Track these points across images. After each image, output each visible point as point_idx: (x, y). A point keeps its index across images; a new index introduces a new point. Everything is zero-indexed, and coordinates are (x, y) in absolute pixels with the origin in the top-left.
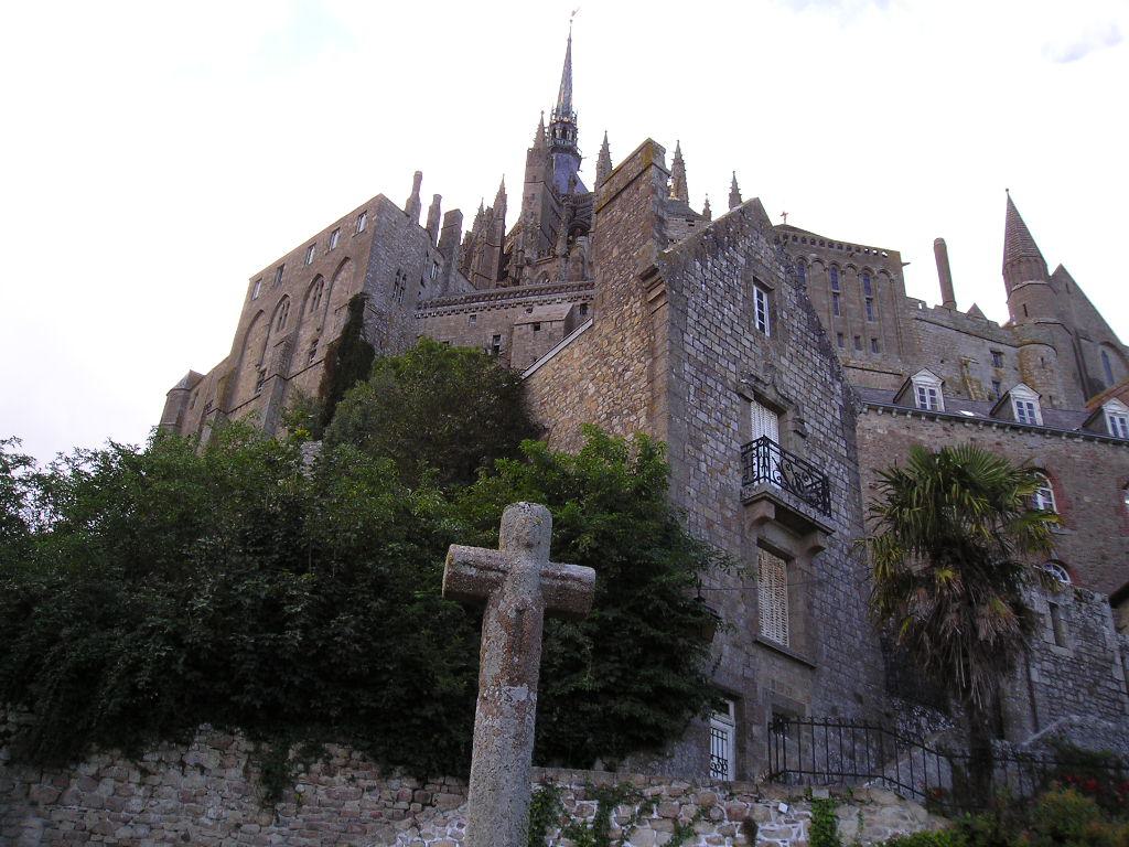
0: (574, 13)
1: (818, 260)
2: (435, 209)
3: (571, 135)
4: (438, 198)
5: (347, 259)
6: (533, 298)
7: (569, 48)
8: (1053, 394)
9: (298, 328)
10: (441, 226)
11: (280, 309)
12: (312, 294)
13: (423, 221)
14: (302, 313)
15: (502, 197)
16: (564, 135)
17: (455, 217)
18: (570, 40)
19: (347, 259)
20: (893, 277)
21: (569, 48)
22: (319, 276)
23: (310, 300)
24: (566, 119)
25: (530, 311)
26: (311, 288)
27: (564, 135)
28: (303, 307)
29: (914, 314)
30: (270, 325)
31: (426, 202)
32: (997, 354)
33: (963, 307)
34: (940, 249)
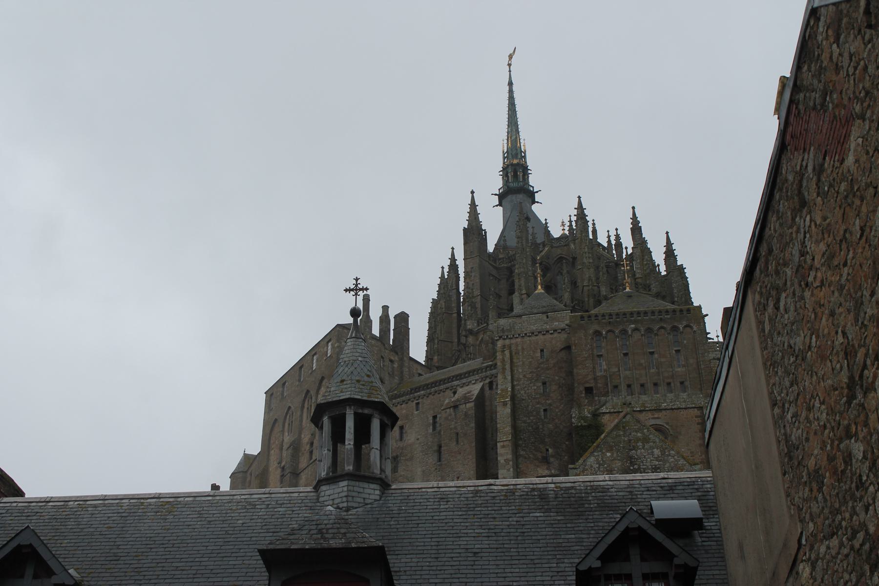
0: (511, 57)
1: (636, 329)
2: (384, 319)
3: (521, 175)
4: (385, 308)
5: (323, 378)
6: (456, 383)
7: (511, 92)
9: (300, 433)
11: (288, 417)
12: (306, 406)
14: (301, 421)
15: (453, 266)
16: (515, 176)
17: (403, 319)
18: (510, 84)
19: (323, 378)
20: (695, 328)
21: (511, 92)
22: (308, 392)
23: (305, 410)
24: (515, 161)
25: (455, 393)
26: (304, 401)
27: (515, 176)
28: (301, 416)
29: (712, 356)
30: (283, 431)
31: (375, 315)
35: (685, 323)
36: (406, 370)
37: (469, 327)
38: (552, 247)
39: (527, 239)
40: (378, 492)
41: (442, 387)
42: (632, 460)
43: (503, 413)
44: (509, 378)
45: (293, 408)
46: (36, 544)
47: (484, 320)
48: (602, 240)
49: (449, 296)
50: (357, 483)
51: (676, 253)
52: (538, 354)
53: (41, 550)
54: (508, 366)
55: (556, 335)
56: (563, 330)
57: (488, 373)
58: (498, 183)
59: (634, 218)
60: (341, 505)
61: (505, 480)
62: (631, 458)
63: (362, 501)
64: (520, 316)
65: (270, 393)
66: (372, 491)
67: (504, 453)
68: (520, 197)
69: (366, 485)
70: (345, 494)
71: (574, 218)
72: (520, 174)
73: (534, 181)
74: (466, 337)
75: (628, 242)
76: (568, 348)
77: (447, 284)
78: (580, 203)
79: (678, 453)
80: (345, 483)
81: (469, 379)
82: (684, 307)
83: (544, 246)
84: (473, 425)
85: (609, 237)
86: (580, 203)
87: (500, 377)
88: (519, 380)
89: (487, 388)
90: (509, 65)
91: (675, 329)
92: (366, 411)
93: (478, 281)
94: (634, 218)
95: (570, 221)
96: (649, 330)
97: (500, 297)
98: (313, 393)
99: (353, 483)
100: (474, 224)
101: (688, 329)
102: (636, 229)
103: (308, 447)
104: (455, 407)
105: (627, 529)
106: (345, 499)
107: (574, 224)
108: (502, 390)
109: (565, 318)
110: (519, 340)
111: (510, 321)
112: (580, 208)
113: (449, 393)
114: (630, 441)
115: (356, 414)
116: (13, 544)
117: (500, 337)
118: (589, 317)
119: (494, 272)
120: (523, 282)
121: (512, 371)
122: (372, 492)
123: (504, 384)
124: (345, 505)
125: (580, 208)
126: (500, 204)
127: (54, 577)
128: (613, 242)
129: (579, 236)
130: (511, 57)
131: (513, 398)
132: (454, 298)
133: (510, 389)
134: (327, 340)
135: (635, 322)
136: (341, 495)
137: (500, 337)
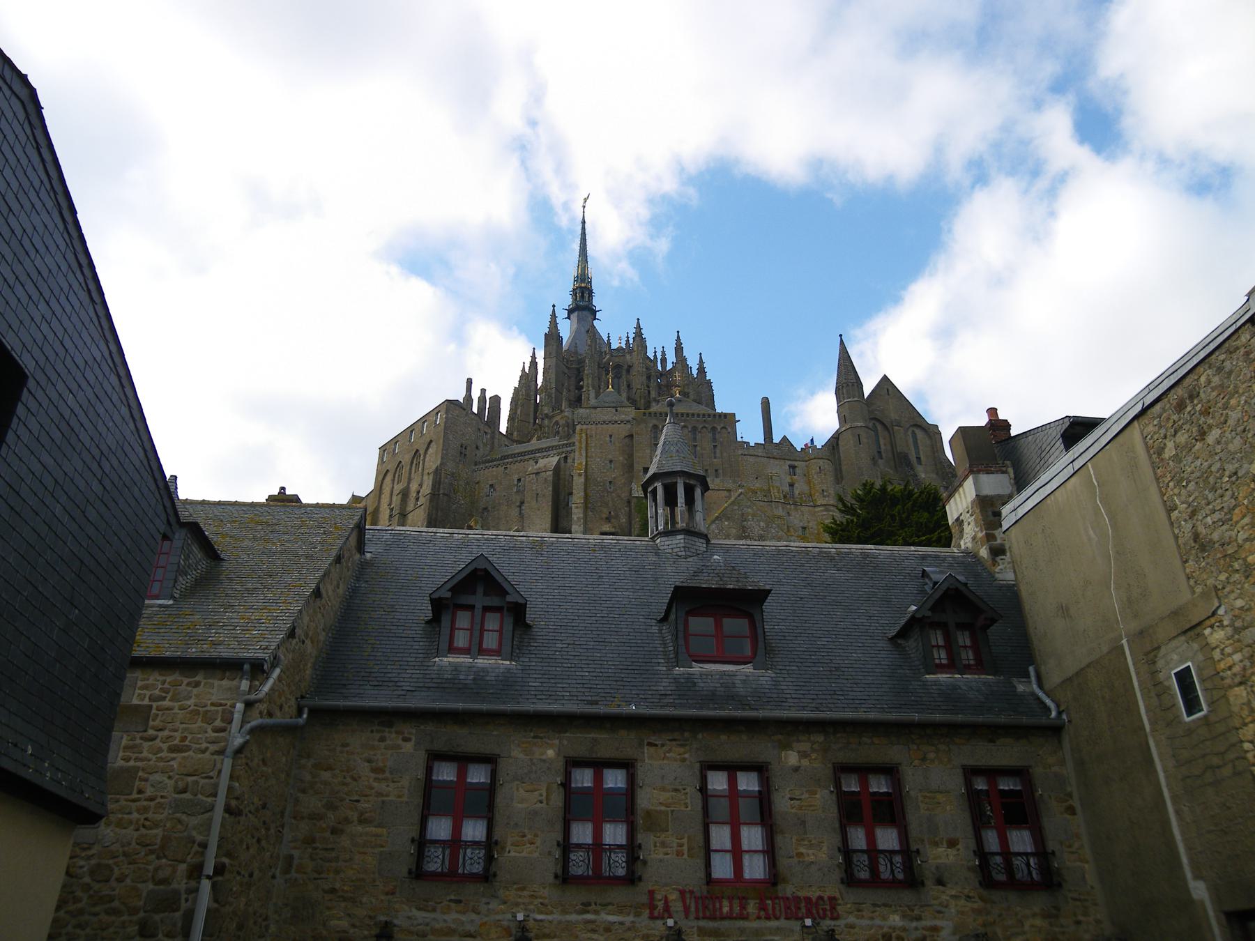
0: (585, 200)
4: (483, 391)
5: (431, 441)
8: (825, 488)
9: (409, 483)
10: (487, 406)
13: (475, 410)
14: (410, 473)
15: (534, 363)
16: (582, 296)
17: (496, 400)
18: (584, 222)
19: (431, 441)
20: (729, 430)
21: (584, 229)
22: (417, 451)
23: (414, 465)
24: (583, 285)
25: (536, 462)
28: (411, 469)
29: (740, 452)
30: (393, 480)
31: (476, 395)
32: (794, 467)
33: (777, 439)
34: (766, 404)
35: (722, 425)
36: (496, 441)
37: (546, 412)
38: (612, 356)
39: (596, 349)
40: (705, 545)
41: (527, 457)
42: (744, 529)
43: (578, 482)
44: (584, 455)
45: (403, 463)
46: (490, 569)
47: (557, 407)
48: (650, 354)
49: (529, 386)
50: (690, 538)
51: (706, 370)
52: (608, 439)
53: (494, 573)
54: (584, 445)
55: (622, 425)
56: (628, 421)
57: (564, 450)
58: (568, 301)
59: (678, 339)
60: (680, 554)
61: (577, 534)
62: (744, 527)
63: (694, 551)
64: (595, 408)
65: (383, 449)
66: (701, 545)
67: (577, 513)
68: (585, 313)
69: (696, 539)
70: (682, 545)
71: (632, 336)
72: (586, 295)
73: (596, 302)
74: (543, 419)
75: (671, 358)
76: (631, 436)
77: (527, 378)
78: (638, 323)
79: (778, 526)
80: (682, 537)
81: (549, 453)
82: (711, 412)
83: (606, 354)
84: (551, 489)
85: (655, 352)
86: (638, 323)
87: (577, 453)
88: (592, 457)
89: (562, 461)
90: (584, 207)
91: (714, 429)
92: (692, 482)
93: (554, 376)
94: (678, 339)
95: (628, 337)
96: (694, 428)
97: (569, 391)
98: (422, 452)
99: (687, 537)
100: (554, 331)
101: (724, 430)
102: (679, 349)
103: (415, 495)
104: (537, 474)
105: (948, 589)
106: (682, 549)
107: (631, 341)
108: (579, 464)
109: (631, 413)
110: (593, 426)
111: (588, 410)
112: (638, 328)
113: (532, 462)
114: (743, 514)
115: (685, 484)
116: (471, 568)
117: (579, 422)
118: (650, 413)
119: (566, 371)
120: (590, 382)
121: (587, 450)
122: (700, 544)
123: (579, 459)
124: (683, 553)
125: (638, 328)
126: (569, 318)
127: (507, 596)
128: (659, 357)
129: (635, 349)
130: (585, 200)
131: (586, 472)
132: (533, 387)
133: (584, 463)
134: (436, 411)
135: (684, 421)
136: (679, 545)
137: (579, 422)
